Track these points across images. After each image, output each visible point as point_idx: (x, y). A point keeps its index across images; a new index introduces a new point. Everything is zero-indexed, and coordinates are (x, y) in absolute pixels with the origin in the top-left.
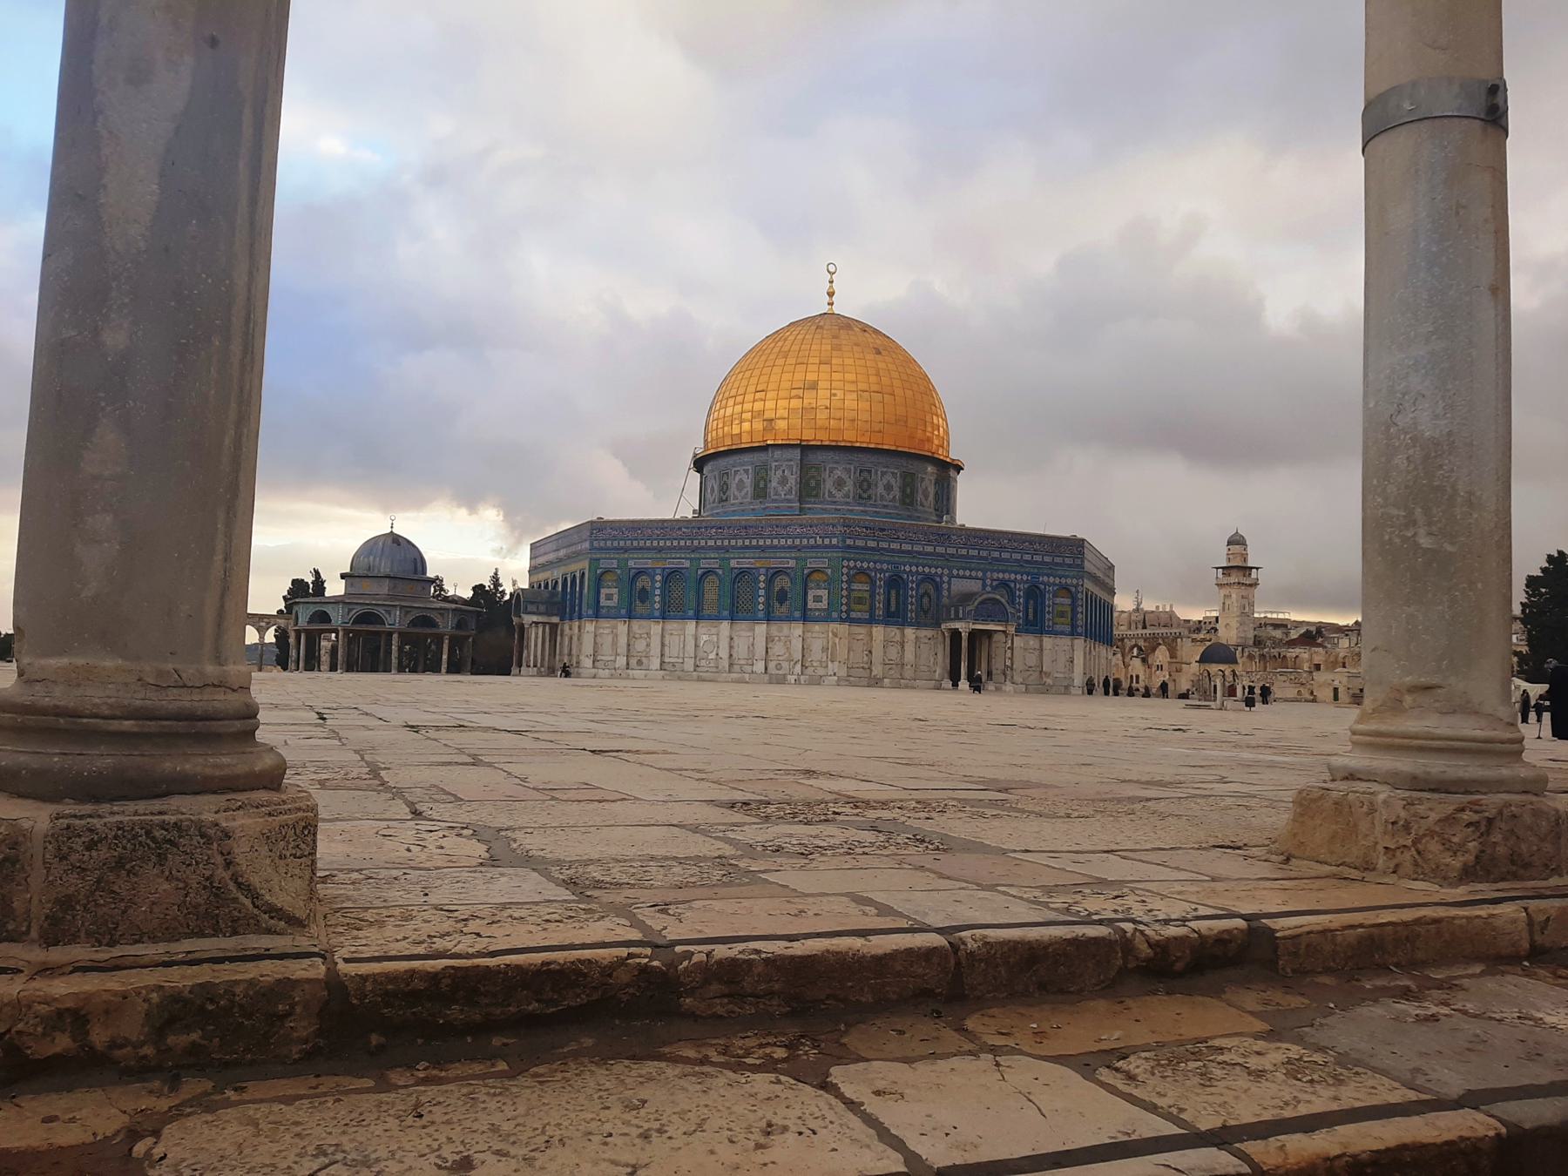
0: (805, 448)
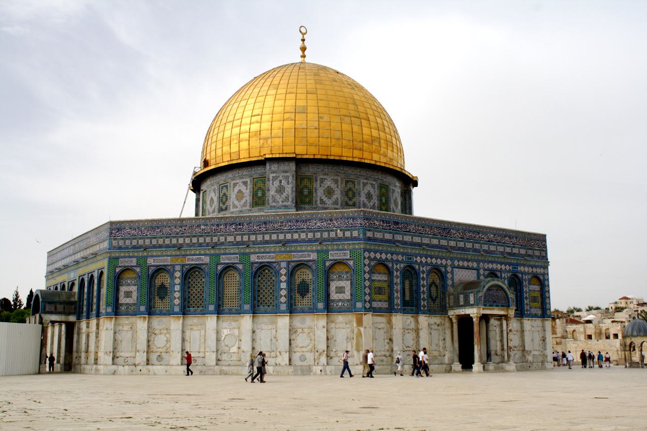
0: (300, 162)
